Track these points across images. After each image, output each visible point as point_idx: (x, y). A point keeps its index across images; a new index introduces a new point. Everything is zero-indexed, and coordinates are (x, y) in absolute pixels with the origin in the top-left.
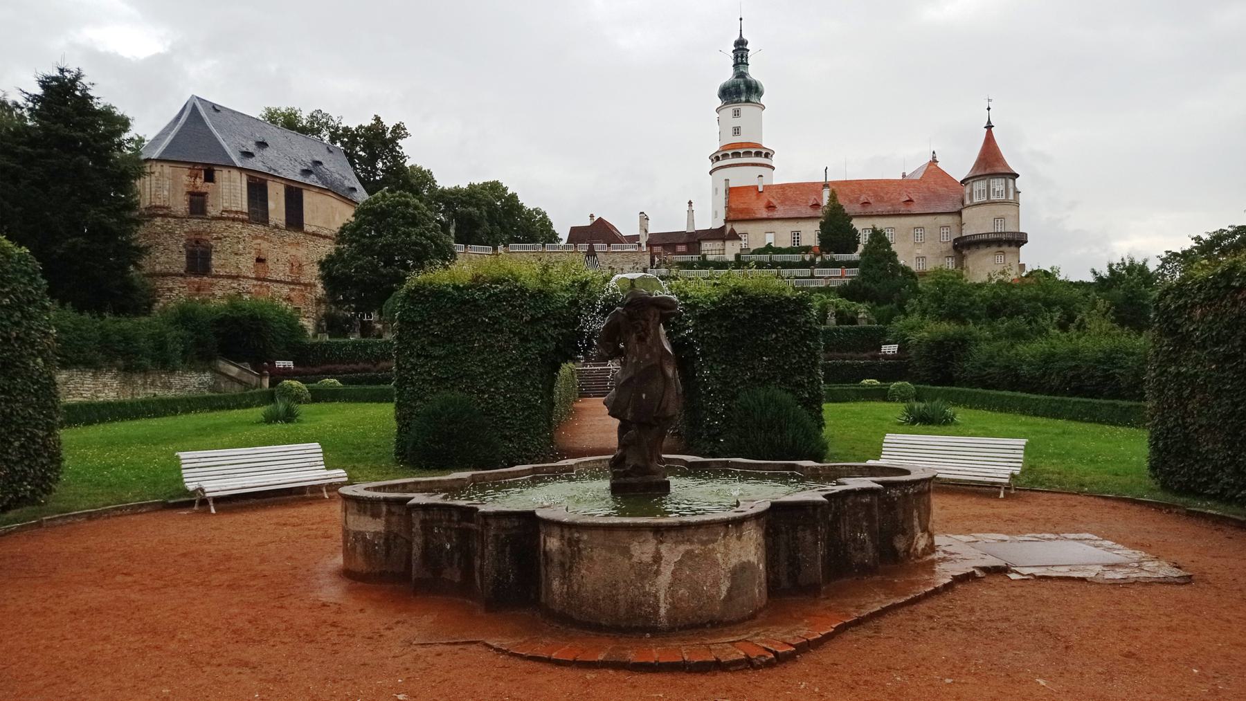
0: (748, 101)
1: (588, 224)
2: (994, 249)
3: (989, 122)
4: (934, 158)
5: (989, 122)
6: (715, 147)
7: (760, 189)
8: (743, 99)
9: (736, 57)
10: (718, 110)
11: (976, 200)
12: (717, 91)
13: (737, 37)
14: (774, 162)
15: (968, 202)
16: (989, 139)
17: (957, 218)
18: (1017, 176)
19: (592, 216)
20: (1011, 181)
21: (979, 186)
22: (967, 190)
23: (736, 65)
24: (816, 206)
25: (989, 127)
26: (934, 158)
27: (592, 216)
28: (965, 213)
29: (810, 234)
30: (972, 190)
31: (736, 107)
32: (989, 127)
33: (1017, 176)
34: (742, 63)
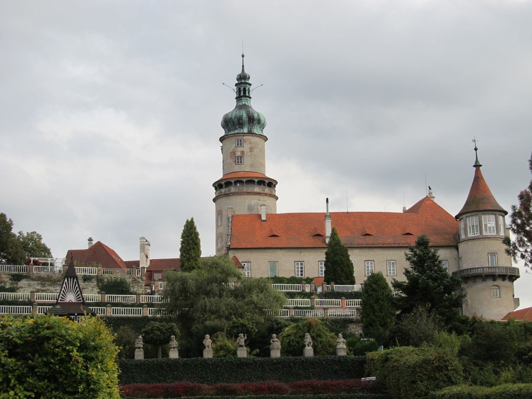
0: (250, 133)
1: (87, 248)
2: (490, 283)
3: (477, 161)
5: (477, 161)
6: (219, 176)
7: (264, 218)
8: (246, 130)
9: (239, 91)
10: (222, 139)
11: (470, 235)
12: (220, 119)
13: (240, 72)
14: (278, 190)
15: (463, 237)
16: (478, 179)
17: (454, 252)
19: (90, 240)
20: (501, 218)
21: (472, 221)
22: (462, 225)
23: (239, 98)
24: (320, 236)
25: (477, 166)
27: (90, 240)
28: (461, 246)
29: (314, 264)
30: (466, 225)
32: (477, 166)
34: (245, 96)
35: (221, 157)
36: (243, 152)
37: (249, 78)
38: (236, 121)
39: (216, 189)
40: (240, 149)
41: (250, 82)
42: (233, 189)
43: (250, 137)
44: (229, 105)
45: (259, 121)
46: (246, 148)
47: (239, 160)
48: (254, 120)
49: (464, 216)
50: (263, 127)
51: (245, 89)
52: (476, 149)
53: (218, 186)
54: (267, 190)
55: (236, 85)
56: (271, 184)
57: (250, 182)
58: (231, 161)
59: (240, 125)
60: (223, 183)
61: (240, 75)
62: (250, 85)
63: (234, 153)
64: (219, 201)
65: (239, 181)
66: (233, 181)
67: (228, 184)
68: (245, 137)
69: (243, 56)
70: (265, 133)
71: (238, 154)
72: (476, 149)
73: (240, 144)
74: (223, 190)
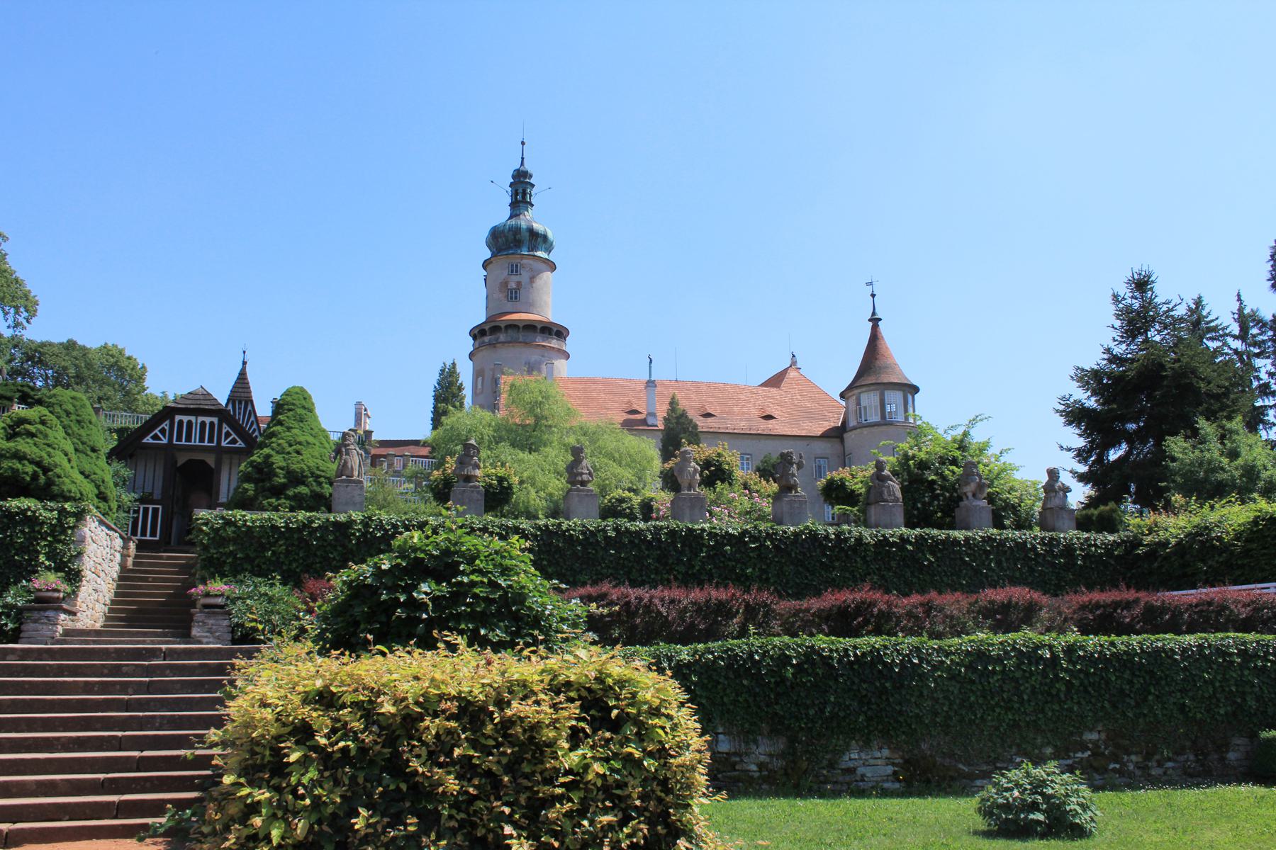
4: (794, 363)
5: (874, 313)
6: (480, 317)
9: (515, 194)
10: (486, 265)
13: (517, 166)
14: (570, 345)
16: (875, 338)
18: (916, 390)
20: (910, 397)
25: (875, 321)
26: (794, 363)
31: (515, 259)
32: (875, 321)
33: (916, 390)
35: (484, 292)
36: (519, 284)
37: (531, 176)
38: (511, 237)
39: (475, 338)
40: (515, 278)
41: (532, 181)
42: (502, 337)
43: (531, 262)
44: (500, 214)
45: (545, 237)
46: (524, 276)
47: (514, 294)
48: (537, 239)
49: (856, 391)
50: (549, 250)
51: (524, 193)
52: (873, 296)
53: (478, 333)
54: (554, 343)
55: (511, 185)
56: (561, 333)
57: (530, 327)
58: (501, 296)
59: (515, 246)
60: (487, 328)
61: (518, 170)
62: (533, 186)
63: (505, 284)
64: (479, 355)
65: (513, 326)
66: (503, 326)
67: (496, 329)
68: (524, 261)
69: (523, 143)
70: (552, 257)
71: (513, 285)
72: (873, 296)
73: (515, 270)
74: (487, 339)
